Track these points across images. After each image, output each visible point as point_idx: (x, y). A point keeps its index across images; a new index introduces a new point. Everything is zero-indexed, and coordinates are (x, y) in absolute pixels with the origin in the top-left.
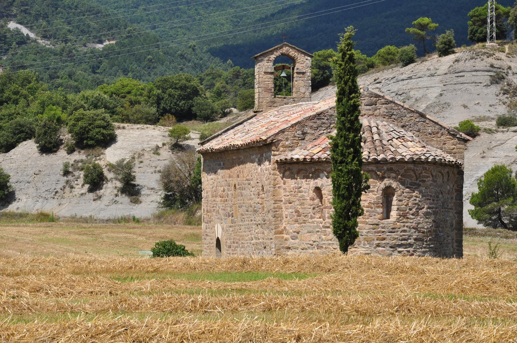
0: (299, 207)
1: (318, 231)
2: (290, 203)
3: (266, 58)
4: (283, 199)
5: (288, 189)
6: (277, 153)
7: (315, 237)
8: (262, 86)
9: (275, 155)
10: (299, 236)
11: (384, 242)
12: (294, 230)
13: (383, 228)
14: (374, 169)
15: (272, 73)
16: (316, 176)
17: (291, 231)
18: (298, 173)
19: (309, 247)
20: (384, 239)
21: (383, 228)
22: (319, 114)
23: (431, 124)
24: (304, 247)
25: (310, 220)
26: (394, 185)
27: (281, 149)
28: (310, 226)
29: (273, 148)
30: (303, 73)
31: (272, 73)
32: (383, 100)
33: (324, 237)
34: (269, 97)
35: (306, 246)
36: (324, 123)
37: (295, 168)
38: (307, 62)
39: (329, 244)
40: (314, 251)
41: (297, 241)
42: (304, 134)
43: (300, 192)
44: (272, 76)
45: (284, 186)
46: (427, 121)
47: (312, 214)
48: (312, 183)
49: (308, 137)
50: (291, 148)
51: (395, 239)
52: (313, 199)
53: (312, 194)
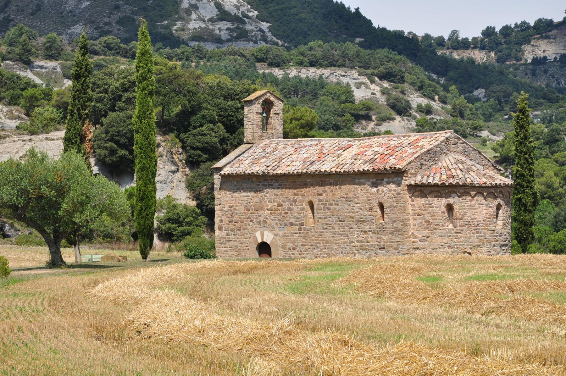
0: (430, 218)
1: (450, 236)
2: (420, 215)
3: (257, 102)
4: (411, 212)
5: (416, 205)
6: (407, 178)
7: (446, 240)
8: (255, 123)
9: (406, 180)
10: (428, 239)
11: (497, 243)
12: (424, 235)
13: (497, 233)
14: (494, 191)
15: (260, 114)
16: (448, 196)
17: (420, 236)
18: (429, 193)
19: (440, 248)
20: (497, 241)
21: (497, 233)
22: (429, 151)
23: (484, 159)
24: (434, 247)
25: (441, 228)
26: (502, 202)
27: (410, 176)
28: (442, 233)
29: (405, 175)
30: (278, 114)
31: (260, 114)
32: (461, 141)
33: (455, 240)
34: (258, 132)
35: (437, 247)
36: (431, 157)
37: (427, 191)
38: (280, 105)
39: (461, 245)
40: (445, 250)
41: (426, 243)
42: (422, 164)
43: (431, 207)
44: (260, 116)
45: (412, 203)
46: (482, 157)
47: (443, 223)
48: (444, 201)
49: (424, 167)
50: (415, 175)
51: (502, 240)
52: (443, 212)
53: (444, 209)
